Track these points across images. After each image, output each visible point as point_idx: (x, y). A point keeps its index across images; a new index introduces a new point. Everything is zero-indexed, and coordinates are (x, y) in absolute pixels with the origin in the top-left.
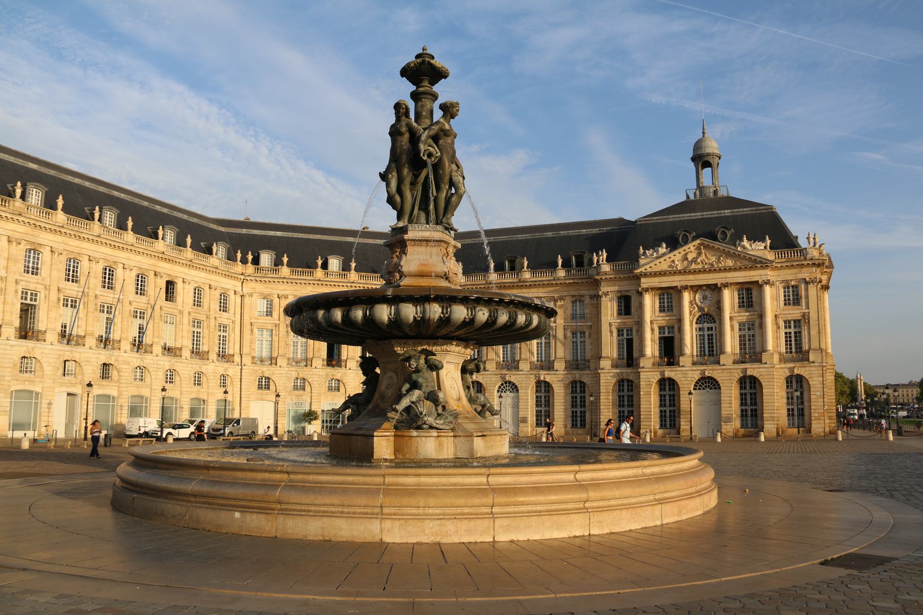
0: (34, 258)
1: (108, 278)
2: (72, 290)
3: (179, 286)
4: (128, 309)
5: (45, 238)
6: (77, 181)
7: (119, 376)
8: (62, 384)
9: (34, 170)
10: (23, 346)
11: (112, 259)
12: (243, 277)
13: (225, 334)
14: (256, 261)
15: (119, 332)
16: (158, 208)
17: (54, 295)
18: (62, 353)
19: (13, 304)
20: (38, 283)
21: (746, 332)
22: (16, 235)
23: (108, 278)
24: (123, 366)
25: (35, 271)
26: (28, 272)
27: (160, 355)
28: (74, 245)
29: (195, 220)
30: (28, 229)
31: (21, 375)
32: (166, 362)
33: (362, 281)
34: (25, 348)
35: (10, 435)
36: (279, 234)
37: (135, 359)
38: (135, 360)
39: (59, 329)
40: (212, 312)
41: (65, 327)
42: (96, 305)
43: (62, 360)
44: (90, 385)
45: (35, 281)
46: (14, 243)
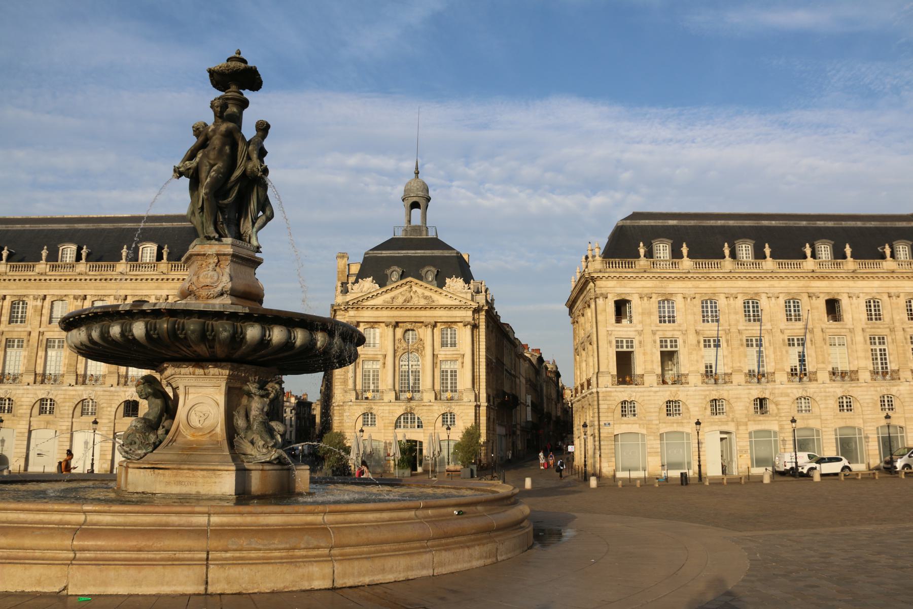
0: (669, 307)
1: (752, 311)
2: (710, 329)
3: (845, 303)
4: (781, 338)
5: (674, 287)
6: (720, 223)
7: (778, 409)
8: (712, 423)
9: (673, 226)
11: (752, 291)
13: (882, 347)
15: (773, 364)
16: (820, 224)
17: (692, 338)
18: (707, 393)
19: (652, 354)
20: (674, 330)
22: (646, 291)
23: (752, 311)
24: (780, 399)
25: (672, 320)
26: (665, 322)
27: (828, 381)
28: (705, 286)
31: (669, 417)
32: (838, 389)
35: (663, 473)
37: (796, 389)
38: (795, 391)
39: (703, 370)
40: (897, 324)
41: (711, 367)
42: (741, 340)
43: (708, 400)
44: (698, 423)
46: (645, 299)
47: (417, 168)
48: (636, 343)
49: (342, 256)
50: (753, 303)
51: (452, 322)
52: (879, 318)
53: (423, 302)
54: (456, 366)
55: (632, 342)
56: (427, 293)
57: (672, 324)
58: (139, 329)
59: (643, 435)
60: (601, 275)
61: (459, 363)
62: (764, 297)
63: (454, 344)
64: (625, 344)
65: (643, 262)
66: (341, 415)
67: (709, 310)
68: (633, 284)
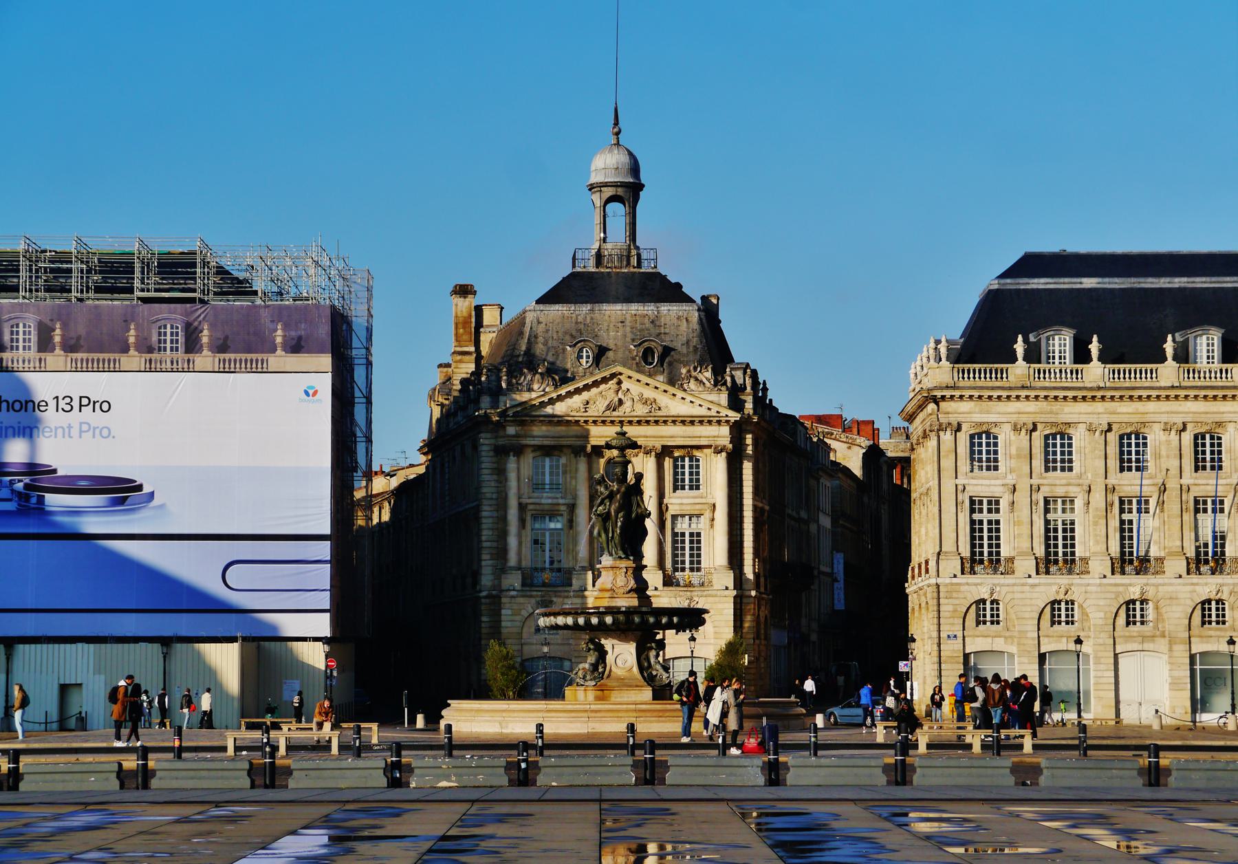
10: (1050, 584)
17: (1098, 498)
22: (1024, 419)
26: (1055, 469)
28: (1125, 413)
30: (1042, 405)
34: (1055, 588)
45: (1064, 482)
47: (616, 123)
48: (1004, 505)
49: (464, 291)
50: (1212, 438)
51: (693, 447)
53: (641, 410)
54: (701, 525)
55: (997, 503)
56: (649, 393)
57: (1067, 473)
58: (609, 620)
59: (1011, 656)
60: (948, 393)
61: (704, 520)
63: (695, 486)
64: (985, 507)
65: (1019, 370)
66: (496, 614)
67: (1130, 450)
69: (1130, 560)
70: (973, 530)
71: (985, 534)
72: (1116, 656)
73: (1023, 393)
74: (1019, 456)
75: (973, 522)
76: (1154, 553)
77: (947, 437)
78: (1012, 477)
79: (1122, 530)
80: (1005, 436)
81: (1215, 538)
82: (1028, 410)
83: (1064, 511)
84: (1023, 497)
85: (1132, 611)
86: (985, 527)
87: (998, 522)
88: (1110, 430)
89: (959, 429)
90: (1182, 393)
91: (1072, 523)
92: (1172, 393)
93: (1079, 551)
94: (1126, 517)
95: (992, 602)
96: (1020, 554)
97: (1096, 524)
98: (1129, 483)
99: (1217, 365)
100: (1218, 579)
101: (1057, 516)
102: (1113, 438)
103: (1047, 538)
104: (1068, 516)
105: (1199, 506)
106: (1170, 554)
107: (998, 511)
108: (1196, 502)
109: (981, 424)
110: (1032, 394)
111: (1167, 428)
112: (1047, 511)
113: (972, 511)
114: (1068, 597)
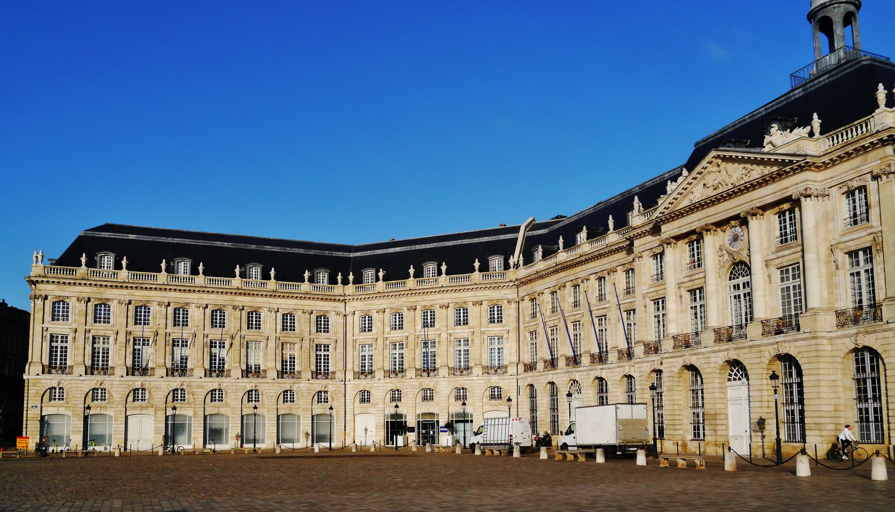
11: (182, 301)
12: (342, 298)
14: (358, 280)
17: (122, 337)
21: (791, 283)
22: (84, 295)
23: (180, 317)
26: (100, 322)
28: (139, 296)
29: (312, 252)
33: (453, 284)
36: (398, 249)
48: (70, 339)
52: (293, 329)
55: (67, 338)
62: (193, 306)
64: (59, 339)
67: (141, 314)
68: (71, 288)
69: (137, 368)
70: (51, 351)
71: (59, 354)
72: (126, 417)
73: (83, 282)
74: (79, 314)
75: (51, 347)
76: (150, 365)
77: (39, 302)
78: (75, 323)
79: (134, 354)
80: (72, 303)
81: (182, 359)
82: (86, 291)
83: (104, 343)
84: (80, 335)
85: (136, 394)
86: (59, 350)
87: (66, 348)
88: (130, 303)
89: (46, 298)
90: (168, 287)
91: (108, 349)
92: (163, 287)
93: (110, 364)
94: (137, 347)
95: (60, 388)
96: (77, 364)
97: (120, 350)
98: (137, 331)
99: (188, 275)
100: (182, 379)
101: (100, 345)
102: (132, 308)
103: (93, 357)
104: (106, 346)
105: (174, 343)
106: (159, 366)
107: (66, 342)
108: (174, 341)
109: (59, 297)
110: (88, 283)
111: (160, 304)
112: (94, 343)
113: (52, 341)
114: (102, 387)
